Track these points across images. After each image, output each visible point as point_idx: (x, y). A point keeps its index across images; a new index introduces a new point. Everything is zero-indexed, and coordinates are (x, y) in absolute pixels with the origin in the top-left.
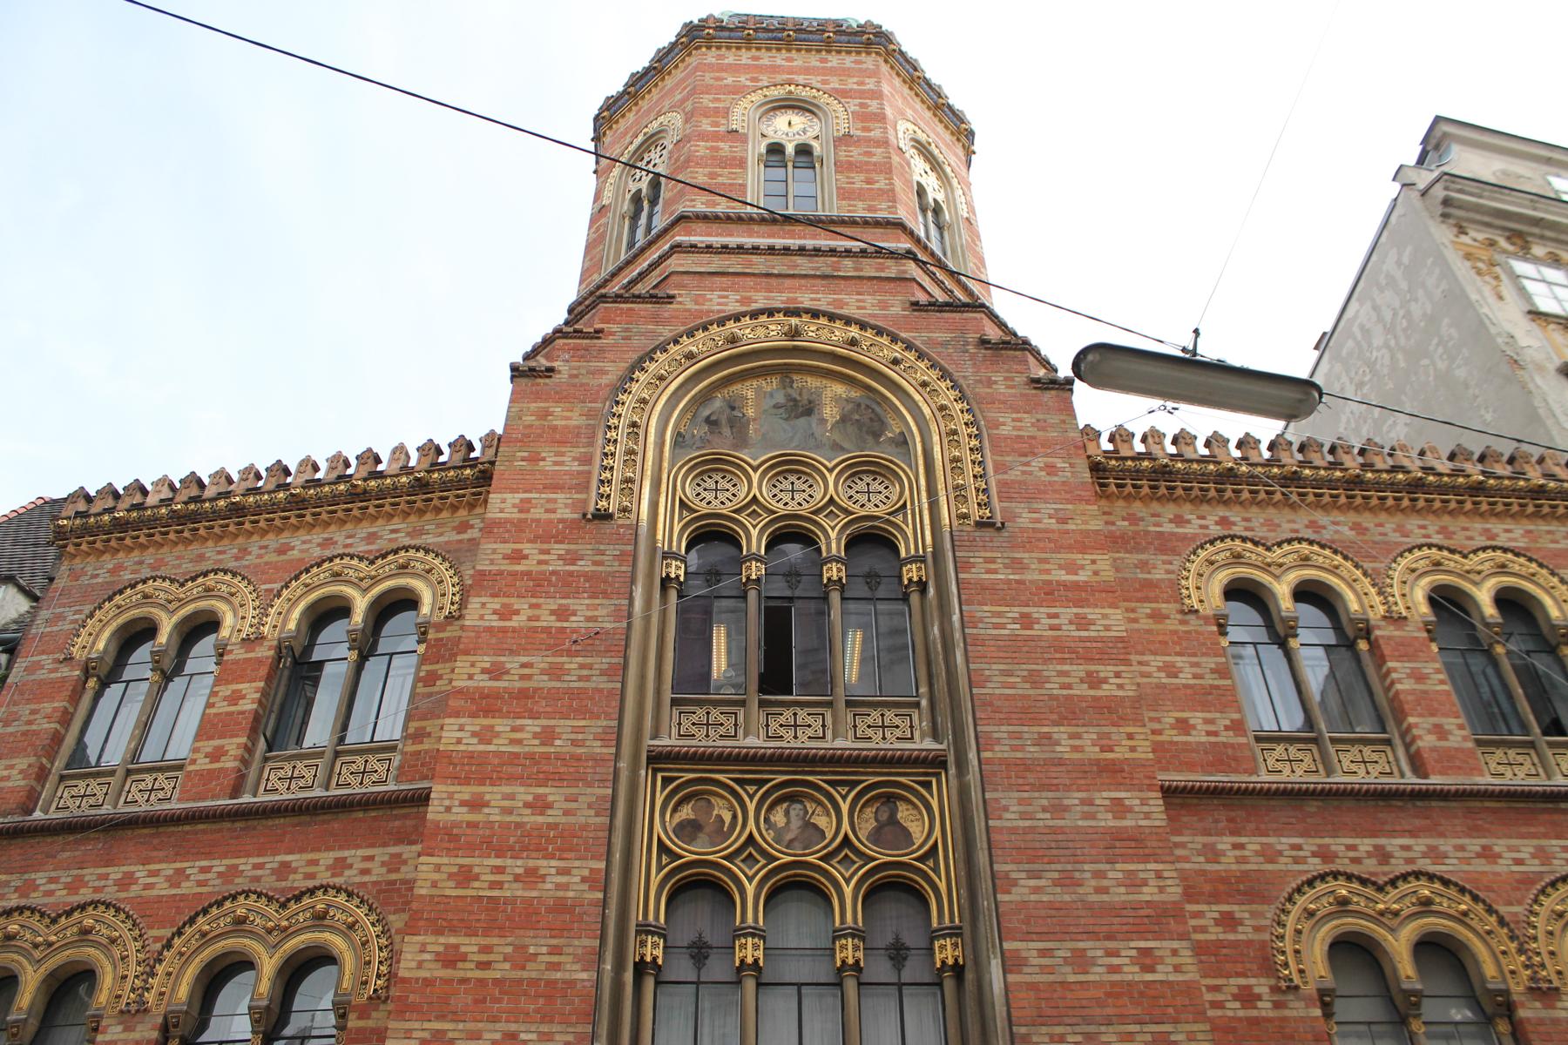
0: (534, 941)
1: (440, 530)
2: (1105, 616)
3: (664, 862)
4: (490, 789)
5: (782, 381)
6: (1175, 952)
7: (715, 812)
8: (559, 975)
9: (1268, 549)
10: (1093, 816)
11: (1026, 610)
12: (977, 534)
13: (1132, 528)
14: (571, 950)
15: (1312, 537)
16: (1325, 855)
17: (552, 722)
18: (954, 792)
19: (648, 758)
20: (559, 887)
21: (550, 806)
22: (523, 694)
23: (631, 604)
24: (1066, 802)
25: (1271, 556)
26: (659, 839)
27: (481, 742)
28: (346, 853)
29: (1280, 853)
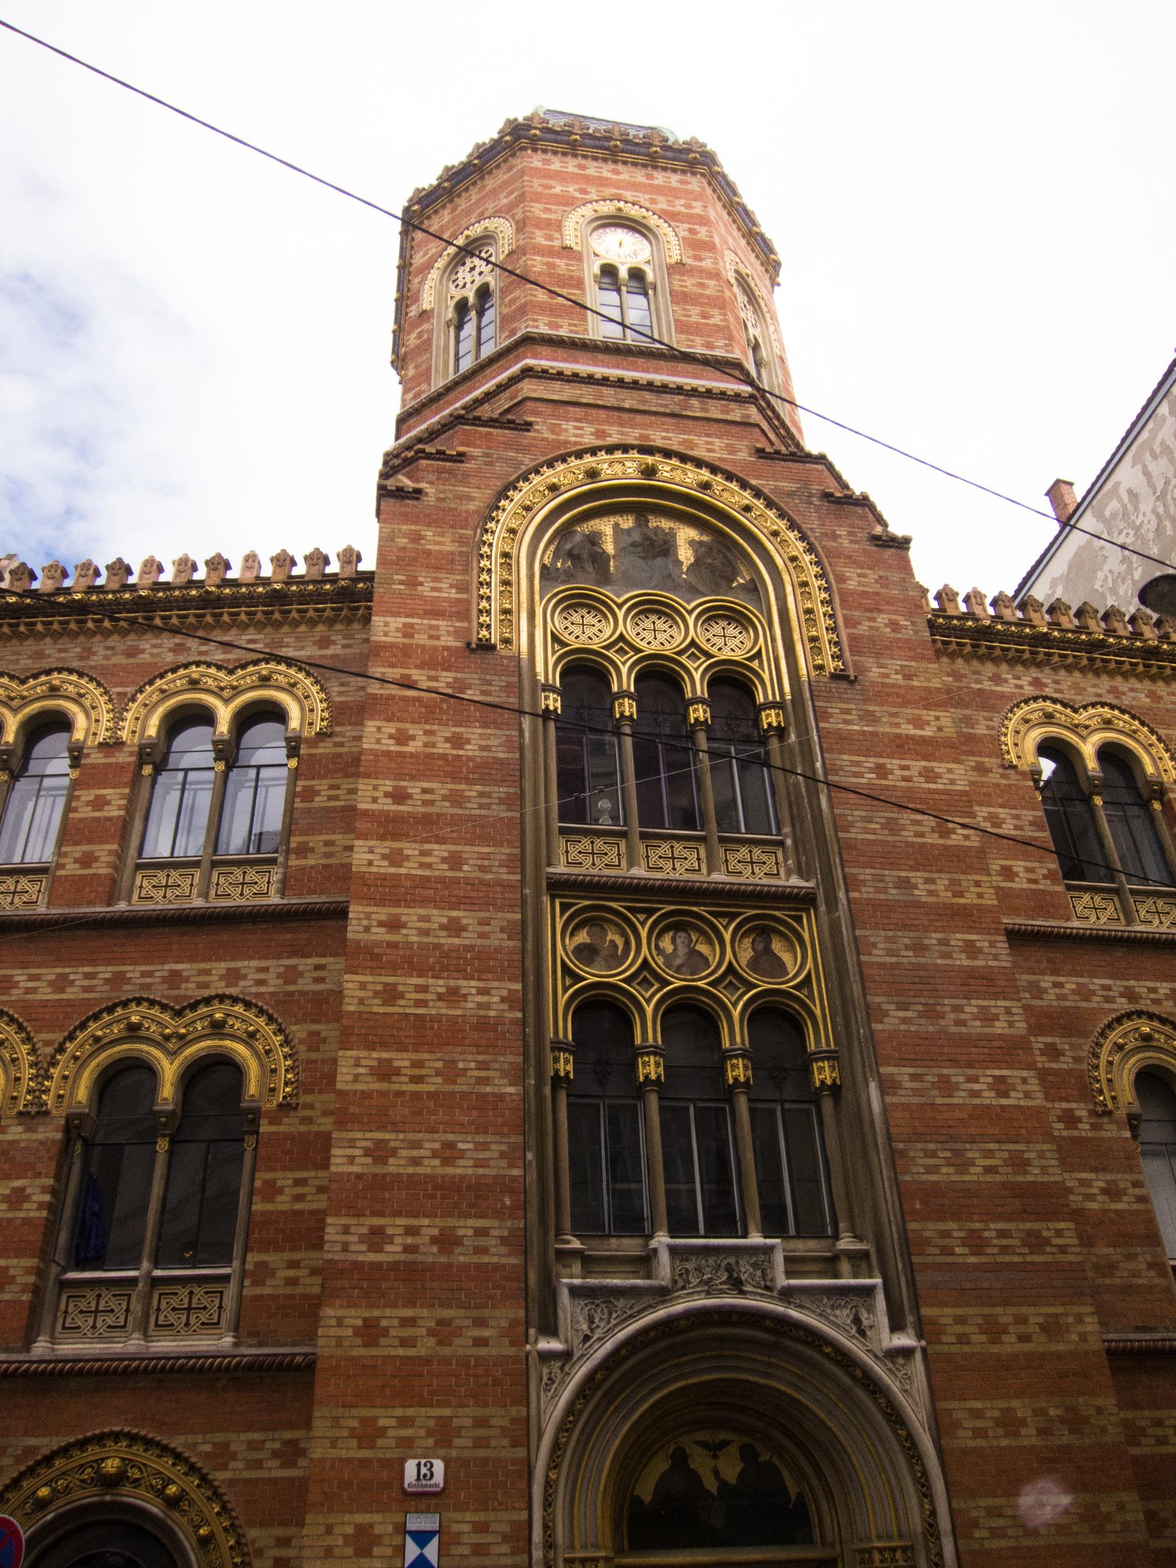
0: (462, 1057)
1: (301, 644)
2: (950, 771)
3: (568, 983)
4: (406, 911)
5: (637, 520)
6: (1024, 1081)
7: (609, 937)
8: (488, 1089)
9: (1075, 711)
10: (948, 955)
11: (881, 761)
12: (833, 685)
13: (956, 684)
14: (497, 1066)
15: (1114, 702)
16: (1131, 996)
17: (459, 848)
18: (826, 928)
19: (549, 885)
20: (480, 1006)
21: (464, 929)
22: (428, 820)
23: (521, 735)
24: (926, 942)
25: (1082, 717)
26: (562, 961)
27: (392, 864)
28: (239, 964)
29: (1093, 993)
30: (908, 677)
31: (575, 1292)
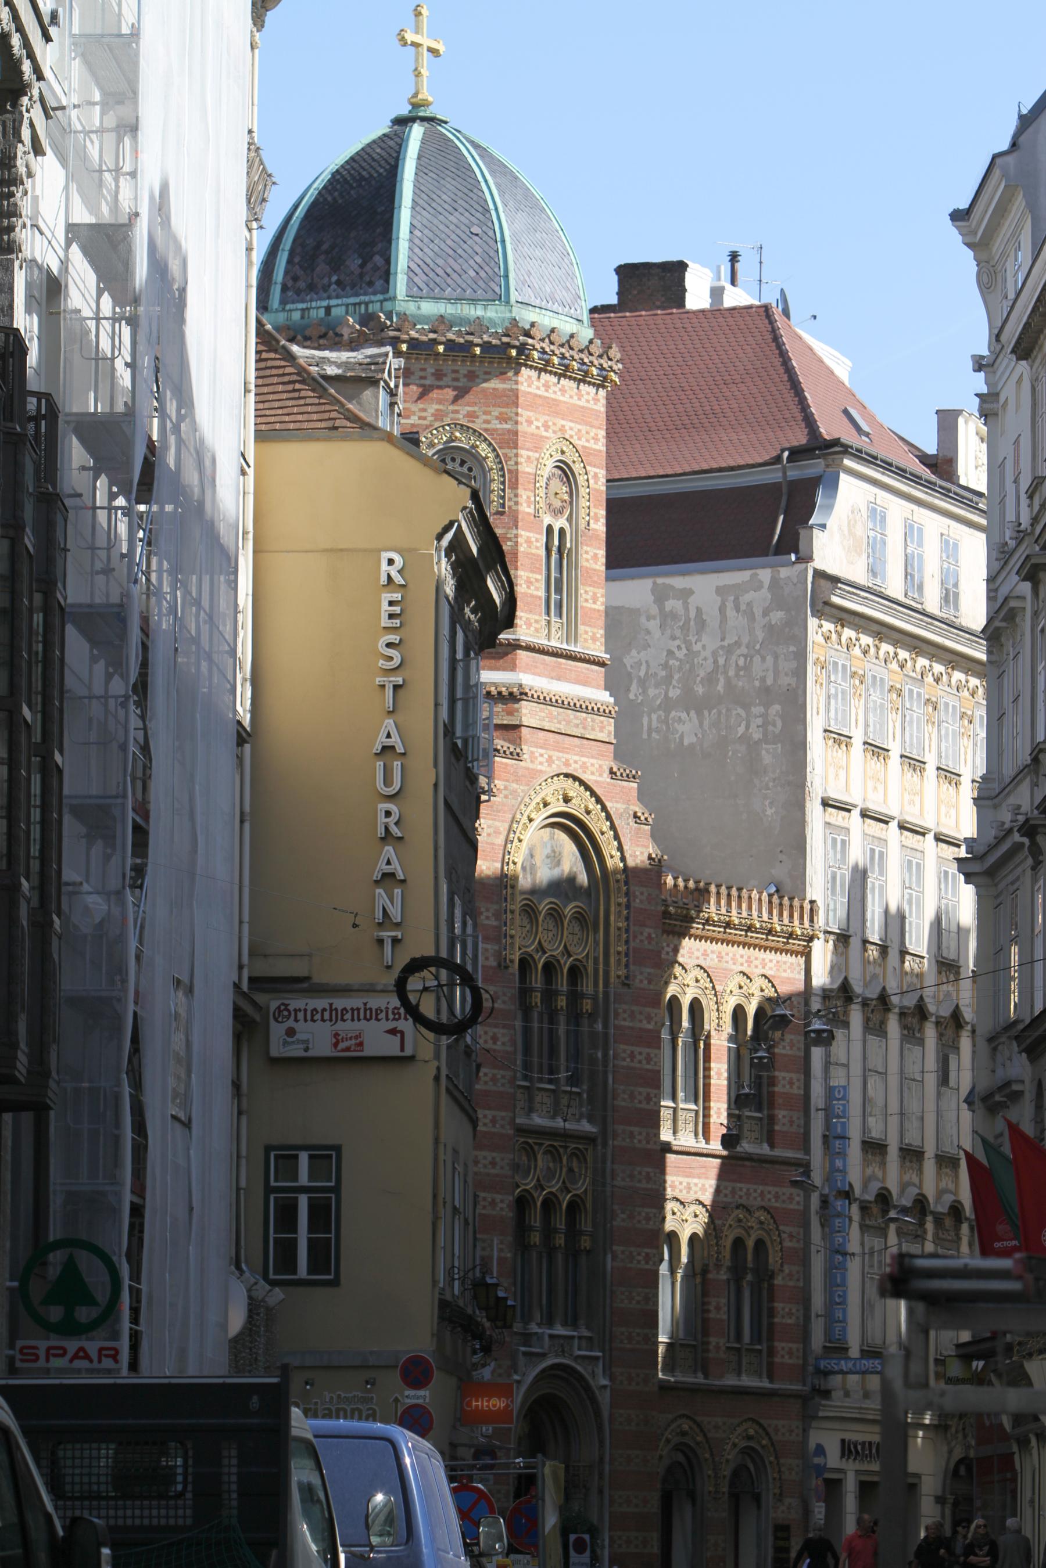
30: (649, 983)
31: (525, 1354)
